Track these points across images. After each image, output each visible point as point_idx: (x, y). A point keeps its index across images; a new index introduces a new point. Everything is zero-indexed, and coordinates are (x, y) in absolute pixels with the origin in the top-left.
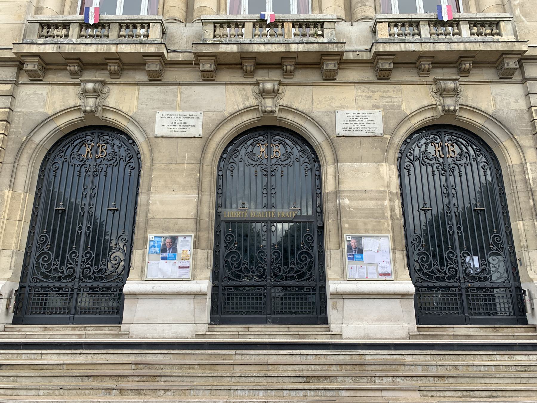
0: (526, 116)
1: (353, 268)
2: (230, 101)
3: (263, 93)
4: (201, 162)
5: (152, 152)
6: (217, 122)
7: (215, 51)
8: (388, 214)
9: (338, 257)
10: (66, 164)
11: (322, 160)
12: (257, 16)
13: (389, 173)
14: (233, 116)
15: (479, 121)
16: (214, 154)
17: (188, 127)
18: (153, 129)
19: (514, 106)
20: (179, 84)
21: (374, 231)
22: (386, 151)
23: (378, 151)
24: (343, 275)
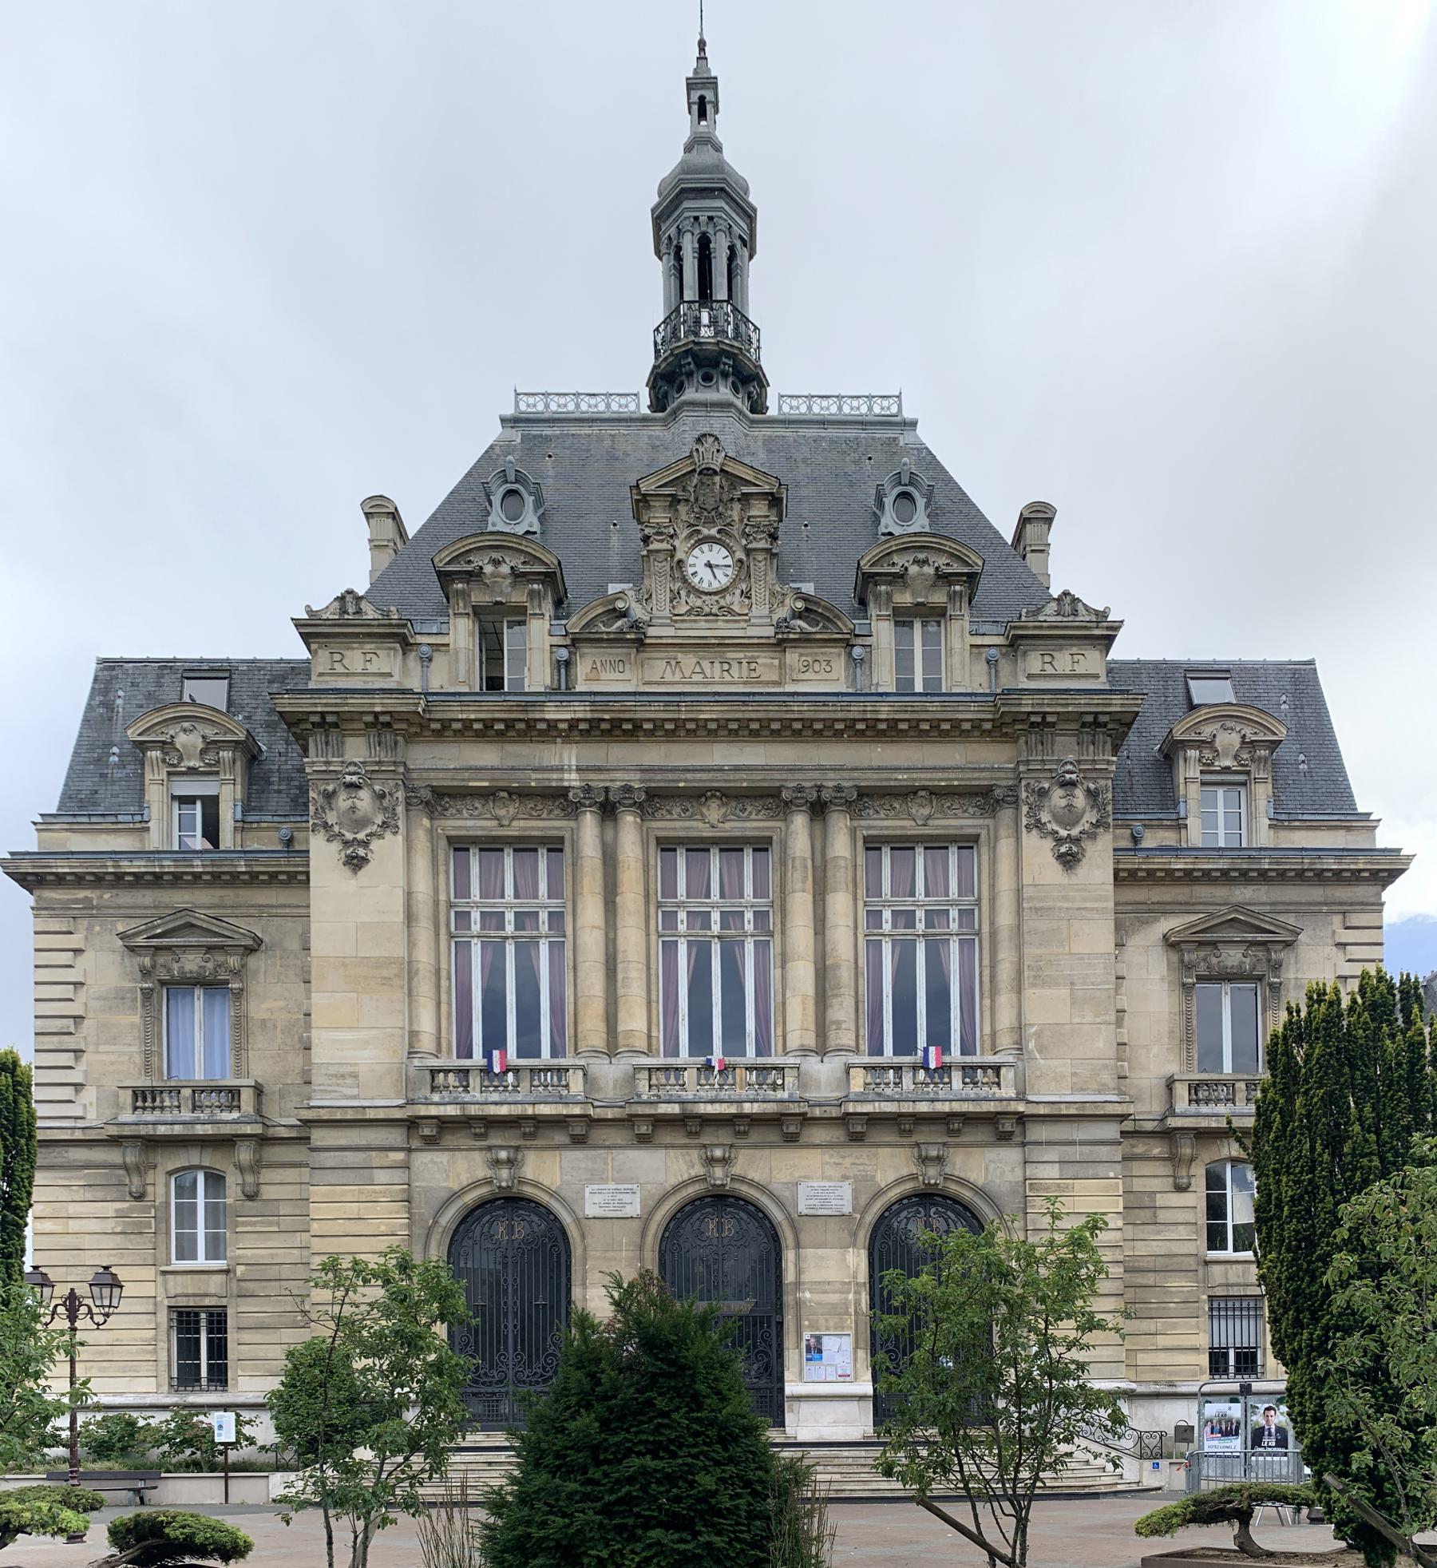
0: (1021, 1190)
1: (812, 1369)
2: (670, 1169)
3: (711, 1161)
4: (641, 1248)
5: (583, 1237)
6: (657, 1198)
7: (653, 1112)
8: (852, 1310)
9: (797, 1357)
10: (477, 1247)
11: (783, 1245)
12: (702, 1060)
13: (857, 1261)
14: (676, 1189)
15: (966, 1194)
16: (655, 1236)
17: (623, 1204)
18: (583, 1210)
19: (1009, 1177)
20: (609, 1147)
21: (836, 1329)
22: (855, 1234)
23: (845, 1234)
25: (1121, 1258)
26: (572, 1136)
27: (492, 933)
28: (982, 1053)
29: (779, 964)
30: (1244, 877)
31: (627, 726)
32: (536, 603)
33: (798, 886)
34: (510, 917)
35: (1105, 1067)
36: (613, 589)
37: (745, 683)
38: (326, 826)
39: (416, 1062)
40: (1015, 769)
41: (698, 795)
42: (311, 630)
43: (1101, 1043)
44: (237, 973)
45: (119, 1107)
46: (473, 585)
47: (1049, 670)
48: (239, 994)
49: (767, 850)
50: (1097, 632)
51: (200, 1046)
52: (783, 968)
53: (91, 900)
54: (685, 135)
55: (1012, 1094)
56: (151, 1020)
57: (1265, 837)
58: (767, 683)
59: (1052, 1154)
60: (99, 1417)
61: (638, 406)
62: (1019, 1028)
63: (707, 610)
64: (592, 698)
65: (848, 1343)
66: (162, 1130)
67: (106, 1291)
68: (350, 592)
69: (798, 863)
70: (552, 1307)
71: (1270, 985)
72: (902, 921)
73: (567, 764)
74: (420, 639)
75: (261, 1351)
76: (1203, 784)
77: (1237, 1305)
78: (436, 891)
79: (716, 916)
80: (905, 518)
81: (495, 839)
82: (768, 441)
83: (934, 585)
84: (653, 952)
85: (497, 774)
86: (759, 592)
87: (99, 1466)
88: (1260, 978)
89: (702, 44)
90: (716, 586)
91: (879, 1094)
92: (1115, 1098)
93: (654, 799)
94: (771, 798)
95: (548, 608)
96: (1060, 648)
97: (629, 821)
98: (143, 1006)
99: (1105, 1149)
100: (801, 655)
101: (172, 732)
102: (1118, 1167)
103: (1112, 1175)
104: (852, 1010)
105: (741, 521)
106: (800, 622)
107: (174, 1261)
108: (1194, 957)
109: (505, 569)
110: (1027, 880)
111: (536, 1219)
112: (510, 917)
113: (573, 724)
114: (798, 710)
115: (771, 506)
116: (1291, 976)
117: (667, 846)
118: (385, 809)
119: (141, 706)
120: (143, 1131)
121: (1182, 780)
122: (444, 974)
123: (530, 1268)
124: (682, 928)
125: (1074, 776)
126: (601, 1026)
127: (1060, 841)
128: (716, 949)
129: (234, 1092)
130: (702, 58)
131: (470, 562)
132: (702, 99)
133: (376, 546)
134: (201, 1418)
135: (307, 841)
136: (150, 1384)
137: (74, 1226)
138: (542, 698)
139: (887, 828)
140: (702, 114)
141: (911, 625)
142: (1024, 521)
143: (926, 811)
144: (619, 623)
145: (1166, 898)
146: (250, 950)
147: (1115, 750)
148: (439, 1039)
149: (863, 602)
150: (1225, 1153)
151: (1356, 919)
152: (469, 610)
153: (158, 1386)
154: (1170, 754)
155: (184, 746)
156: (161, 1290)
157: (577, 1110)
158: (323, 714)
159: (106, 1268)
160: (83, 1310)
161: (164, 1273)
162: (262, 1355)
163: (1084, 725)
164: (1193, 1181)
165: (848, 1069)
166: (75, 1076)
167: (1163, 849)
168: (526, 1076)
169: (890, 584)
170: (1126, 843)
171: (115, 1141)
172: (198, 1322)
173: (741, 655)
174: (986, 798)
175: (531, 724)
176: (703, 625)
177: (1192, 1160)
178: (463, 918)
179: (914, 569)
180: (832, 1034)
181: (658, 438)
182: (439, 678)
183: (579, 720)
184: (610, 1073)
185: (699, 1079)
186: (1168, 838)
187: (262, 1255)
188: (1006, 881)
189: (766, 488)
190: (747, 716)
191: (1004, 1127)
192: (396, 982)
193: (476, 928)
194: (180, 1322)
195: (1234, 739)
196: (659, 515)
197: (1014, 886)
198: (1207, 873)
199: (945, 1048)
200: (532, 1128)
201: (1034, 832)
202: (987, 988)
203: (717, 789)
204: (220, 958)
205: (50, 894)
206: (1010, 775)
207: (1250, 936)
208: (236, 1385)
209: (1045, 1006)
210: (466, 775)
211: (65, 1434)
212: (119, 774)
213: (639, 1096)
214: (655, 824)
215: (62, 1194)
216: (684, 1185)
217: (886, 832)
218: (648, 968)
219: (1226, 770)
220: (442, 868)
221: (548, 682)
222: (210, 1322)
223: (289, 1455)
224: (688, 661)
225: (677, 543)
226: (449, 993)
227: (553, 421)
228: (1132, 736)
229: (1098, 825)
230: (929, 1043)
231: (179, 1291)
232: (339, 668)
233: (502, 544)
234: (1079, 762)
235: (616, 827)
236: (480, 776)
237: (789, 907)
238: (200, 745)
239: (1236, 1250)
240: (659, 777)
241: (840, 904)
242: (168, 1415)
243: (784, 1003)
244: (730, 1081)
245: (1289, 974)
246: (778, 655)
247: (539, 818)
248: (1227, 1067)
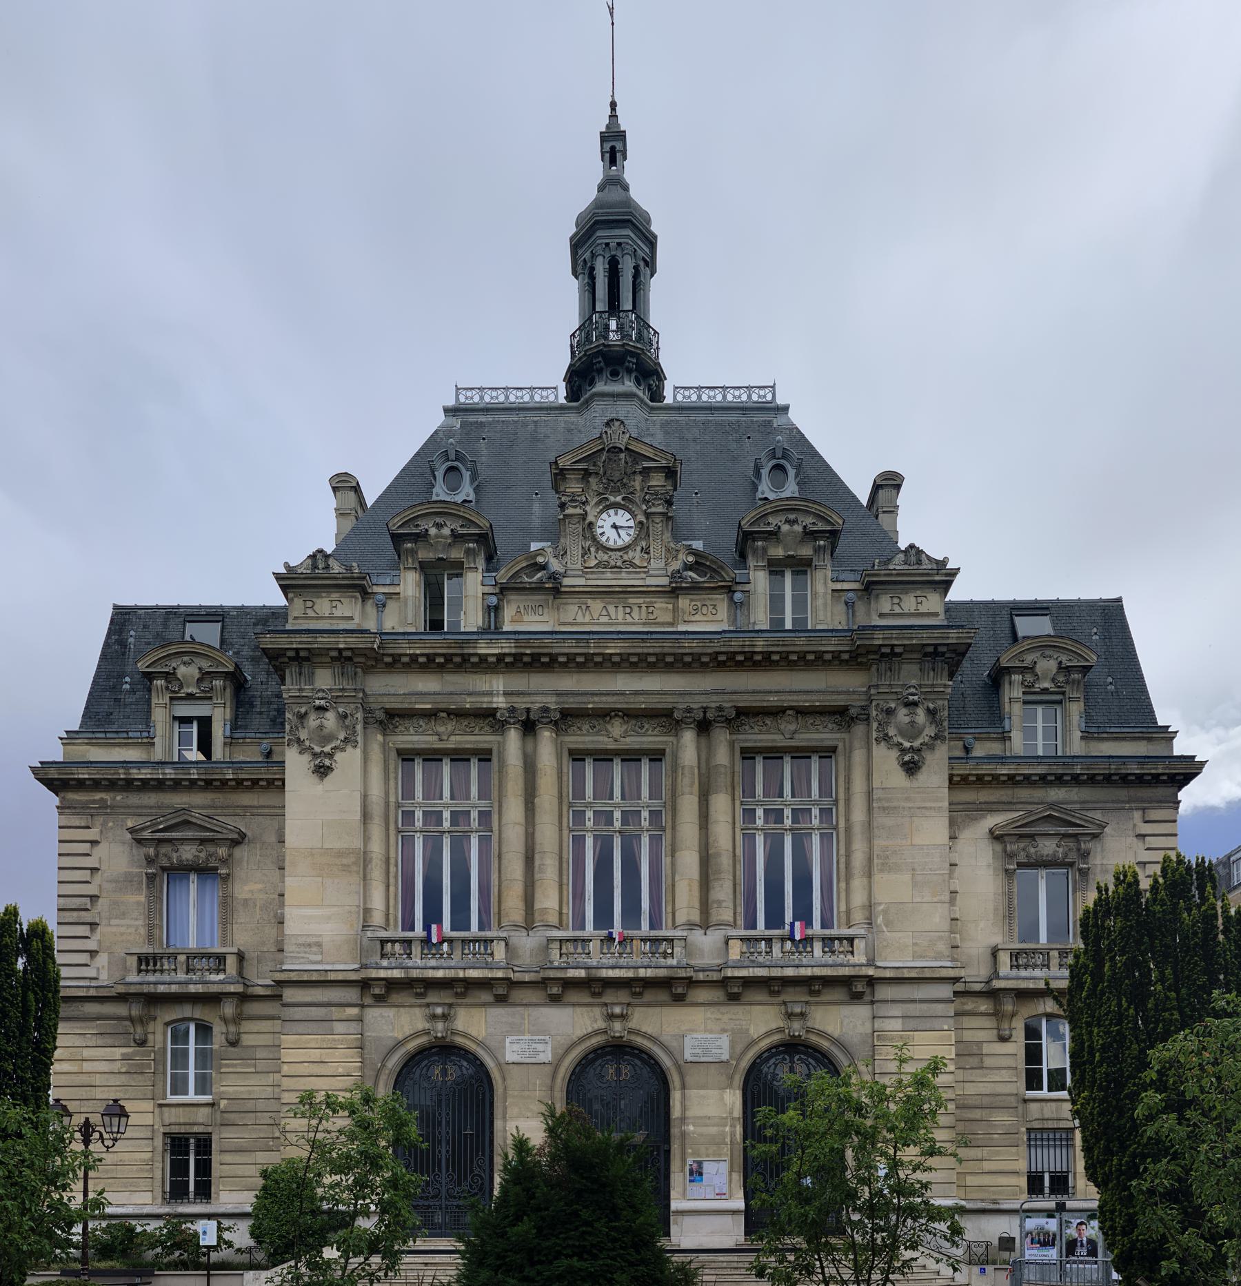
0: (870, 1040)
1: (694, 1189)
2: (577, 1023)
3: (611, 1017)
4: (552, 1089)
8: (728, 1140)
9: (681, 1179)
10: (417, 1087)
12: (605, 933)
13: (733, 1100)
14: (582, 1039)
15: (825, 1044)
17: (537, 1052)
20: (526, 1005)
21: (714, 1155)
22: (731, 1078)
24: (684, 1195)
25: (953, 1097)
26: (496, 996)
27: (432, 828)
28: (839, 927)
29: (669, 853)
30: (1059, 780)
31: (545, 660)
32: (471, 559)
33: (687, 790)
34: (446, 815)
35: (941, 938)
36: (534, 546)
37: (644, 624)
38: (299, 742)
39: (369, 934)
40: (867, 692)
41: (605, 715)
42: (289, 582)
43: (937, 919)
45: (126, 970)
46: (420, 545)
47: (897, 610)
48: (226, 879)
49: (660, 760)
50: (937, 578)
51: (194, 920)
52: (673, 856)
53: (106, 801)
54: (598, 176)
55: (863, 960)
56: (154, 898)
57: (1077, 747)
58: (663, 624)
59: (896, 1010)
60: (104, 1224)
61: (556, 397)
62: (870, 907)
63: (613, 563)
64: (517, 636)
65: (724, 1167)
66: (161, 989)
67: (115, 1120)
68: (320, 551)
69: (686, 771)
70: (478, 1136)
71: (1080, 870)
72: (772, 818)
73: (495, 690)
74: (376, 589)
75: (240, 1170)
76: (1025, 703)
77: (1051, 1136)
78: (387, 794)
79: (617, 815)
80: (778, 485)
81: (436, 751)
82: (664, 425)
83: (802, 541)
84: (565, 844)
85: (439, 699)
86: (657, 549)
87: (102, 1265)
88: (1071, 865)
89: (613, 105)
90: (620, 543)
91: (753, 961)
92: (949, 964)
93: (566, 718)
94: (665, 717)
95: (481, 563)
97: (546, 736)
98: (148, 887)
99: (940, 1006)
100: (692, 600)
101: (174, 665)
102: (951, 1021)
103: (946, 1027)
104: (730, 891)
105: (642, 490)
106: (690, 573)
107: (169, 1095)
108: (1015, 847)
109: (446, 531)
111: (465, 1064)
112: (446, 815)
113: (500, 657)
114: (689, 646)
115: (667, 477)
116: (1098, 862)
117: (577, 756)
118: (347, 727)
119: (149, 643)
120: (146, 989)
121: (1007, 700)
122: (392, 861)
123: (460, 1105)
124: (589, 824)
125: (916, 698)
126: (520, 905)
127: (904, 751)
128: (617, 842)
129: (221, 959)
130: (613, 116)
131: (417, 526)
132: (613, 148)
133: (341, 514)
134: (189, 1225)
135: (283, 754)
136: (146, 1198)
137: (87, 1067)
138: (475, 637)
139: (761, 741)
140: (613, 161)
141: (782, 573)
142: (876, 487)
143: (792, 727)
144: (539, 575)
145: (992, 798)
146: (235, 843)
147: (951, 676)
148: (387, 915)
149: (743, 556)
150: (1041, 1009)
151: (1154, 814)
152: (417, 565)
153: (154, 1199)
154: (998, 677)
155: (184, 676)
156: (158, 1119)
157: (500, 974)
158: (297, 650)
159: (116, 1101)
160: (96, 1135)
161: (161, 1106)
162: (240, 1173)
163: (926, 655)
164: (1014, 1033)
165: (727, 940)
166: (91, 945)
167: (990, 758)
168: (458, 945)
169: (765, 539)
170: (959, 753)
171: (122, 998)
172: (188, 1146)
173: (641, 601)
174: (841, 715)
175: (465, 658)
176: (609, 575)
177: (1013, 1015)
178: (409, 816)
179: (785, 528)
180: (713, 912)
181: (572, 423)
182: (392, 621)
183: (505, 654)
184: (527, 943)
185: (602, 948)
186: (995, 748)
187: (242, 1091)
188: (858, 785)
189: (664, 463)
190: (646, 651)
191: (857, 988)
192: (355, 868)
193: (419, 824)
194: (172, 1146)
195: (1052, 665)
196: (573, 486)
197: (865, 789)
198: (1027, 777)
199: (808, 923)
200: (462, 988)
203: (619, 710)
204: (211, 849)
205: (71, 796)
206: (863, 697)
207: (1063, 830)
208: (218, 1198)
209: (892, 888)
210: (413, 699)
211: (75, 1238)
212: (130, 699)
213: (551, 962)
214: (567, 739)
215: (78, 1041)
217: (759, 745)
218: (561, 858)
219: (1045, 691)
220: (392, 776)
221: (480, 623)
222: (197, 1146)
223: (260, 1256)
224: (596, 605)
225: (588, 508)
226: (396, 877)
227: (487, 410)
228: (966, 664)
229: (936, 738)
230: (795, 918)
231: (173, 1120)
232: (311, 613)
233: (445, 511)
234: (920, 686)
236: (425, 700)
237: (679, 807)
238: (197, 675)
239: (1050, 1090)
240: (571, 700)
241: (721, 804)
242: (161, 1223)
243: (673, 886)
244: (628, 950)
245: (1096, 860)
246: (672, 600)
247: (472, 733)
248: (1043, 938)
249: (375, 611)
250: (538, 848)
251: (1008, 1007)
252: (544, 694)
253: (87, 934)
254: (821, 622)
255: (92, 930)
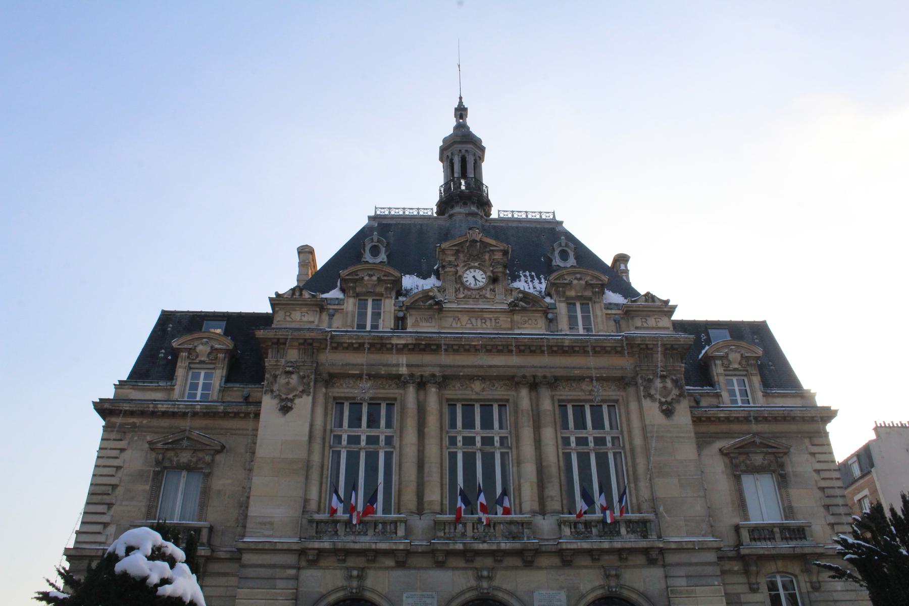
3: (480, 578)
29: (515, 464)
37: (494, 329)
38: (272, 391)
44: (210, 465)
47: (645, 325)
48: (208, 476)
59: (681, 571)
73: (402, 363)
74: (329, 307)
95: (394, 295)
96: (649, 316)
98: (153, 479)
102: (719, 579)
103: (716, 583)
105: (490, 259)
109: (375, 278)
110: (647, 423)
113: (406, 345)
118: (305, 384)
122: (325, 467)
127: (661, 404)
141: (574, 304)
146: (218, 452)
148: (319, 503)
178: (338, 438)
179: (575, 282)
182: (338, 324)
184: (421, 524)
189: (502, 248)
191: (654, 557)
193: (344, 443)
200: (373, 555)
201: (648, 399)
202: (631, 478)
204: (200, 455)
209: (667, 488)
216: (463, 592)
218: (442, 466)
220: (329, 412)
221: (392, 326)
224: (464, 319)
229: (680, 395)
235: (426, 395)
238: (208, 350)
241: (548, 433)
243: (520, 485)
247: (384, 388)
249: (327, 318)
250: (426, 460)
251: (753, 568)
252: (431, 366)
253: (105, 511)
254: (602, 331)
255: (109, 508)
